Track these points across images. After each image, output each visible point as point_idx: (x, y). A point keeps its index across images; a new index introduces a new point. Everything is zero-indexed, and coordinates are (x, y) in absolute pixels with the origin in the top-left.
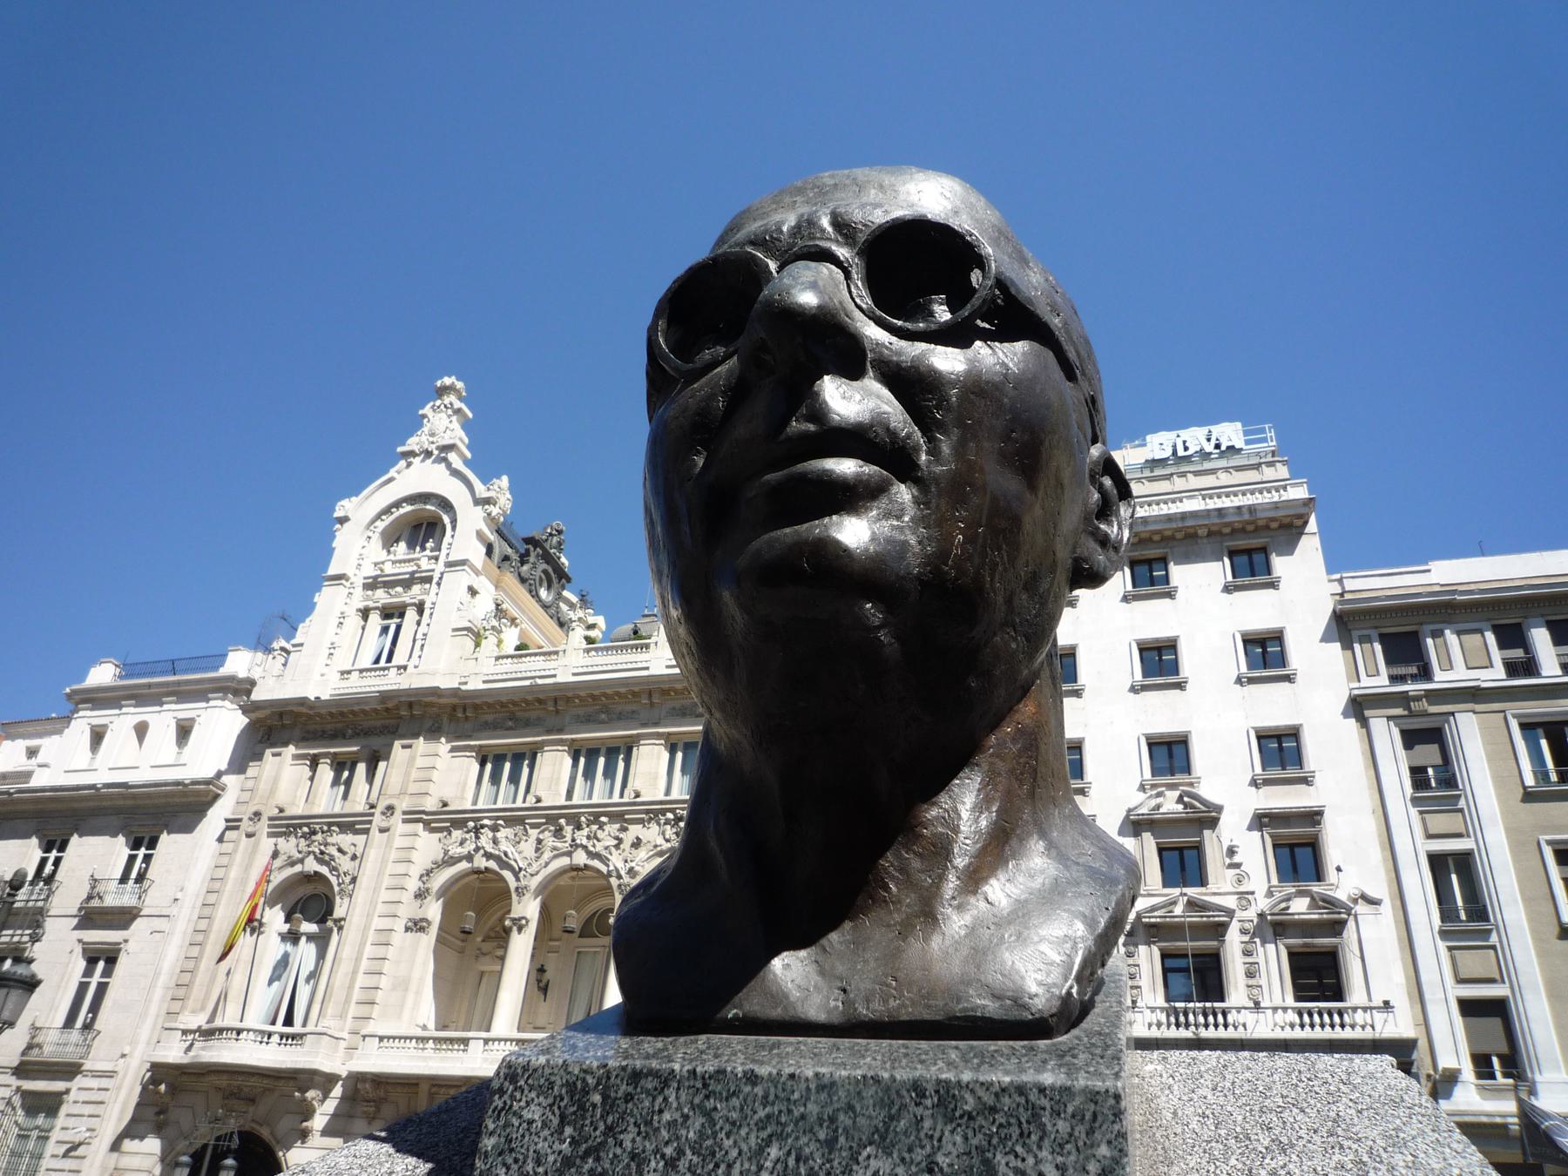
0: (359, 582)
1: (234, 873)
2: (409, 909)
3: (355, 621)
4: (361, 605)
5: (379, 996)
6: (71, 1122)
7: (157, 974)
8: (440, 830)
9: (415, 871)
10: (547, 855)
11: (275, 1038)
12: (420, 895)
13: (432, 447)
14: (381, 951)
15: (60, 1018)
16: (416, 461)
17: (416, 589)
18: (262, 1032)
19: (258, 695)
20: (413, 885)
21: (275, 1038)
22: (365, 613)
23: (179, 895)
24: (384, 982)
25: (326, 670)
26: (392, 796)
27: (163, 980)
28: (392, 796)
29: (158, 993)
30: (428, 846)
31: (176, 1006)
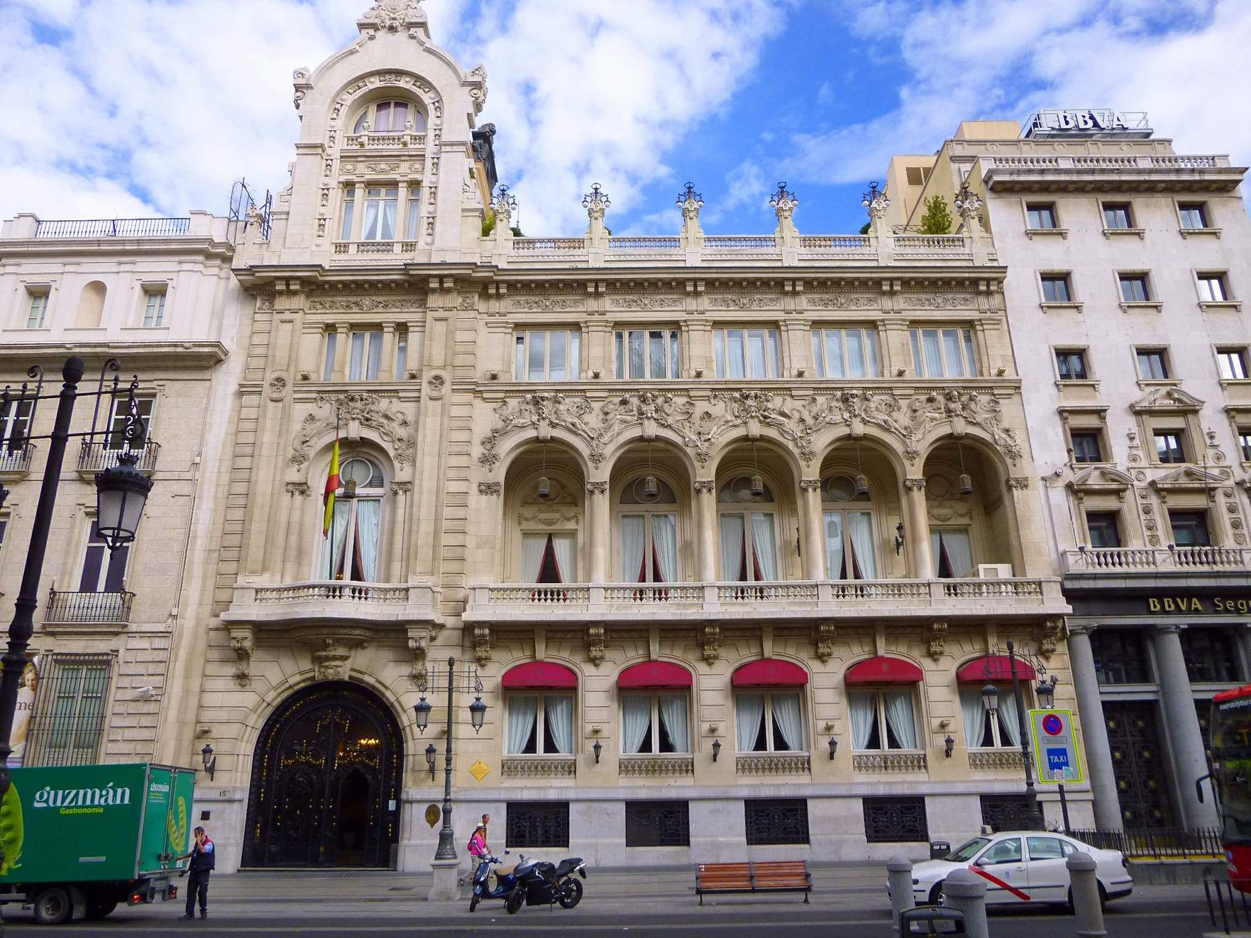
0: (335, 152)
1: (267, 438)
2: (480, 474)
3: (336, 195)
4: (343, 179)
5: (468, 554)
6: (125, 682)
7: (189, 536)
8: (493, 400)
9: (476, 441)
10: (616, 428)
11: (347, 592)
12: (488, 460)
13: (396, 24)
14: (460, 513)
15: (76, 584)
16: (381, 34)
17: (404, 167)
18: (328, 587)
19: (238, 263)
20: (477, 451)
21: (347, 592)
22: (349, 186)
23: (197, 460)
24: (470, 541)
25: (320, 241)
26: (438, 368)
27: (200, 544)
28: (438, 368)
29: (198, 556)
30: (484, 417)
31: (232, 567)
